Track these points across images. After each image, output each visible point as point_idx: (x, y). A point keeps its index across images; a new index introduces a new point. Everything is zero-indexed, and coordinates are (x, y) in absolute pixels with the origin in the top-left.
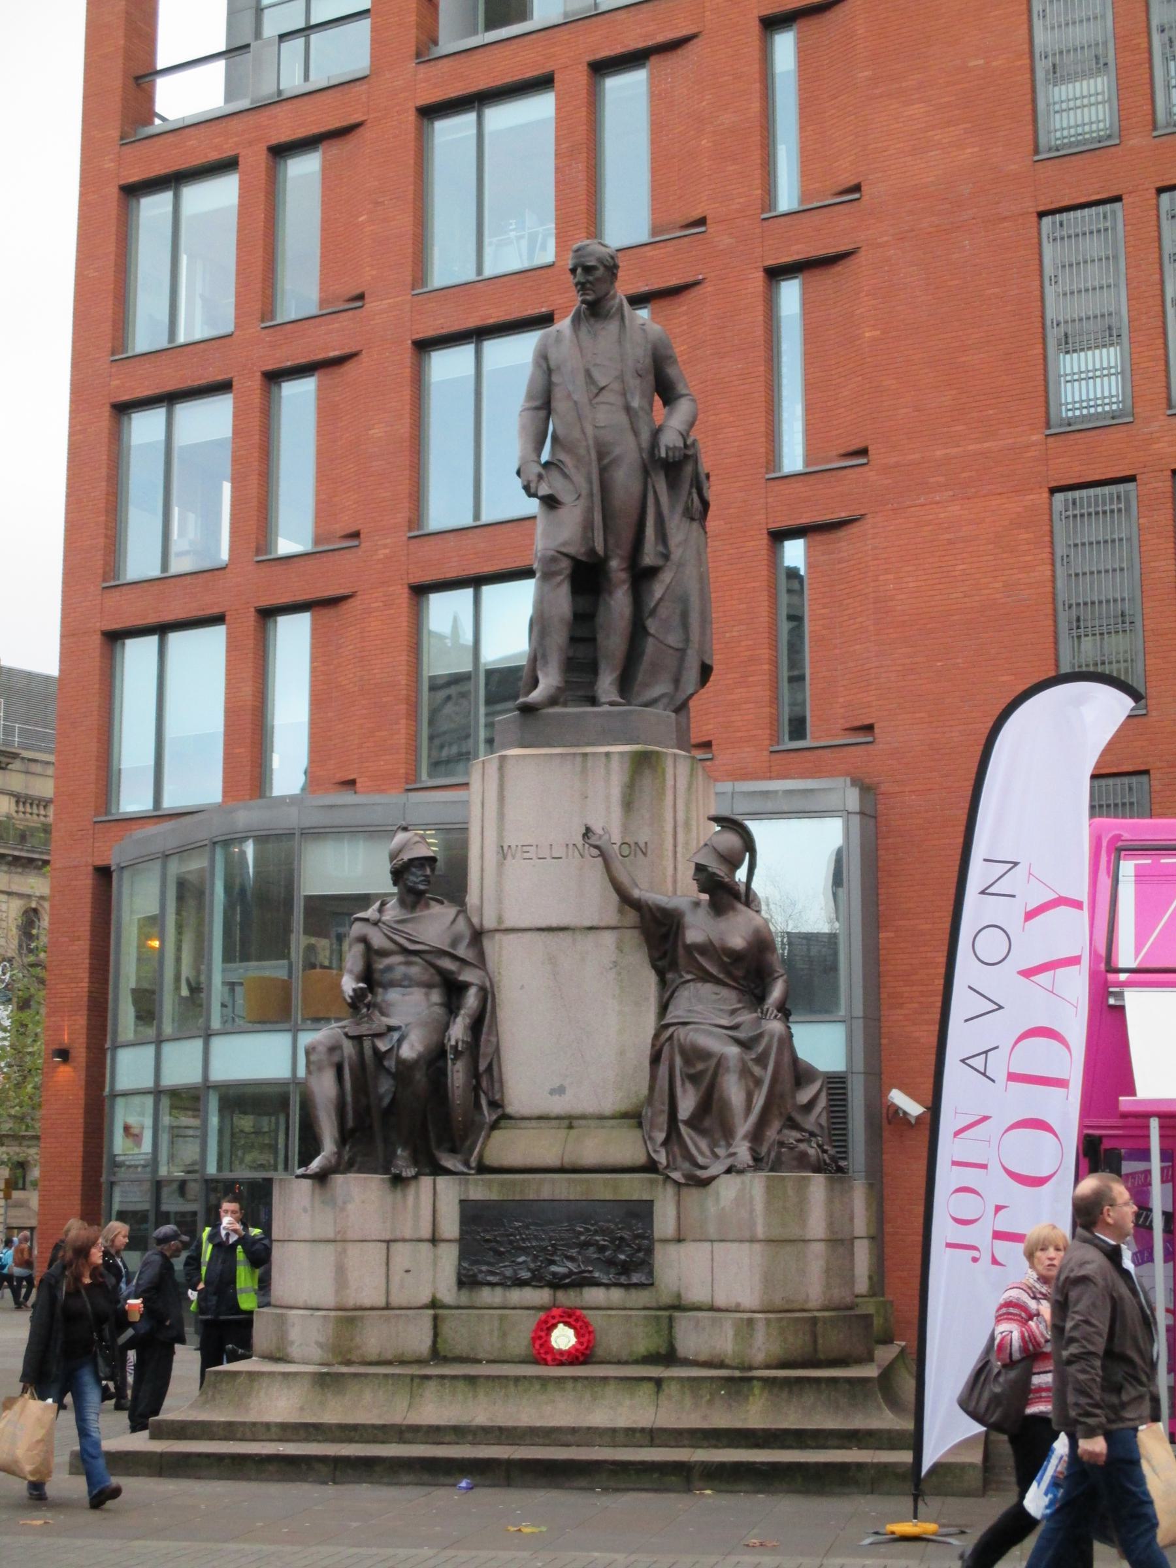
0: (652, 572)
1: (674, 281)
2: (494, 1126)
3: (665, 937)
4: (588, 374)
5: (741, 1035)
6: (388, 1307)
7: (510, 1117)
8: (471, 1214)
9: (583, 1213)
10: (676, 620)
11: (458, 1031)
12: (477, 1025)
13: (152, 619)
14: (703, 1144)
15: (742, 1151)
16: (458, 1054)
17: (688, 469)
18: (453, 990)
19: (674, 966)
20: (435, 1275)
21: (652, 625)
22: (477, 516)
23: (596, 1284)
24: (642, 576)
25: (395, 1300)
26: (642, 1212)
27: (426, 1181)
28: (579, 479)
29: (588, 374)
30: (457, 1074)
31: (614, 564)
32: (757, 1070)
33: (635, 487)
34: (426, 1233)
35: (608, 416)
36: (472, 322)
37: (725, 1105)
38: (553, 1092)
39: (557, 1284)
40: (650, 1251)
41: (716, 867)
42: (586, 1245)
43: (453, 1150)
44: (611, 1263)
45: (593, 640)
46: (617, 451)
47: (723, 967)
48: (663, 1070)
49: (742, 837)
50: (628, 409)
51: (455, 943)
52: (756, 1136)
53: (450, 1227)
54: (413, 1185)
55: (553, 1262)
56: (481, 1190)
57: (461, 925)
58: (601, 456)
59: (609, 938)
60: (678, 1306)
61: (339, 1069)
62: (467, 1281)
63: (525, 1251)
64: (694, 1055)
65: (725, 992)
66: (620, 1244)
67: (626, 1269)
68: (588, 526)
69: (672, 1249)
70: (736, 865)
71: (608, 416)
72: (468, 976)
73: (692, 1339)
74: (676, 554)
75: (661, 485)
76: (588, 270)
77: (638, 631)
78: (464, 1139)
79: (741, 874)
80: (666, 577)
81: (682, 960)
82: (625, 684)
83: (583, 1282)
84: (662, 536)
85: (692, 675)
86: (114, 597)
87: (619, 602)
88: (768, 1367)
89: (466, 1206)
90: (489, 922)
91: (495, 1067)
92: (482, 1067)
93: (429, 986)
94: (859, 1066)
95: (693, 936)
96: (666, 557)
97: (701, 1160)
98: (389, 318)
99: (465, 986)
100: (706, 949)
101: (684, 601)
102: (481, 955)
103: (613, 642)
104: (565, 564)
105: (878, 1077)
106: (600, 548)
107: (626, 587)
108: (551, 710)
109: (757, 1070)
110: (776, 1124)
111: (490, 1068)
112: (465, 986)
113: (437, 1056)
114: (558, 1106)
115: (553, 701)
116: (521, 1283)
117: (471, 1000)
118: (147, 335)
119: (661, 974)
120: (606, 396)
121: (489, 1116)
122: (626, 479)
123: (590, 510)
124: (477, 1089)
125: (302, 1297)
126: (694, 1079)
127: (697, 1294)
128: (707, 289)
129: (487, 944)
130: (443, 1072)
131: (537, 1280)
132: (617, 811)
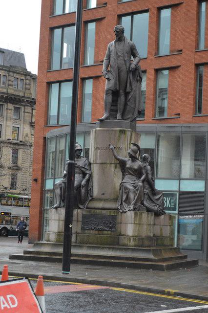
0: (129, 93)
1: (176, 3)
2: (91, 200)
3: (123, 166)
5: (134, 185)
8: (84, 216)
9: (104, 217)
10: (133, 102)
11: (84, 182)
12: (88, 181)
13: (57, 79)
14: (126, 205)
15: (132, 208)
16: (83, 187)
17: (137, 71)
18: (84, 174)
19: (125, 171)
24: (127, 94)
28: (114, 75)
30: (83, 190)
31: (121, 91)
32: (136, 192)
33: (126, 76)
35: (121, 61)
36: (131, 11)
37: (130, 198)
39: (98, 230)
41: (132, 154)
42: (104, 223)
43: (82, 205)
44: (108, 227)
45: (117, 106)
46: (122, 69)
47: (133, 172)
48: (121, 190)
50: (124, 60)
51: (85, 165)
52: (135, 204)
57: (87, 162)
58: (118, 70)
60: (120, 235)
61: (61, 188)
62: (83, 229)
63: (92, 223)
64: (126, 188)
65: (134, 177)
67: (111, 228)
68: (115, 84)
69: (120, 225)
70: (136, 153)
71: (121, 61)
75: (131, 76)
76: (117, 32)
77: (126, 104)
78: (84, 203)
80: (132, 93)
81: (126, 170)
82: (123, 115)
84: (131, 85)
85: (136, 113)
86: (49, 74)
87: (122, 98)
88: (133, 246)
90: (92, 162)
92: (89, 189)
95: (128, 166)
96: (132, 90)
97: (125, 208)
99: (87, 174)
100: (130, 168)
102: (91, 168)
103: (120, 106)
104: (110, 92)
106: (118, 89)
108: (107, 121)
109: (136, 192)
110: (140, 202)
112: (87, 174)
113: (80, 186)
115: (107, 118)
117: (87, 177)
118: (58, 11)
119: (122, 172)
120: (120, 58)
121: (90, 198)
122: (124, 75)
125: (53, 230)
126: (126, 193)
128: (184, 4)
129: (92, 166)
130: (80, 190)
131: (95, 229)
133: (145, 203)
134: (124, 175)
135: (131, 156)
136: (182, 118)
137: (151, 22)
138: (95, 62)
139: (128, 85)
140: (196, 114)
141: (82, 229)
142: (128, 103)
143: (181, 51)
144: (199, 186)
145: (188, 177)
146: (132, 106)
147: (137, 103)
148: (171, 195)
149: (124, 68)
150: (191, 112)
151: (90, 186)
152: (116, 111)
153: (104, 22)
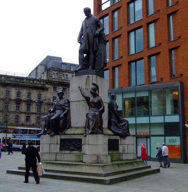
4: (86, 25)
6: (50, 153)
7: (72, 127)
8: (62, 140)
16: (61, 119)
20: (57, 148)
21: (97, 59)
22: (135, 52)
23: (75, 150)
24: (95, 52)
25: (51, 152)
26: (80, 140)
27: (56, 136)
29: (86, 25)
30: (61, 121)
31: (90, 51)
34: (56, 143)
38: (76, 124)
40: (82, 146)
45: (89, 62)
47: (94, 105)
49: (95, 86)
50: (91, 29)
51: (65, 104)
52: (93, 129)
53: (59, 142)
54: (54, 137)
55: (70, 147)
56: (63, 137)
59: (83, 102)
62: (61, 149)
66: (78, 145)
68: (85, 46)
70: (96, 91)
72: (67, 108)
73: (85, 159)
74: (100, 48)
77: (95, 60)
79: (97, 92)
83: (73, 150)
89: (61, 139)
91: (69, 120)
92: (67, 120)
93: (61, 110)
94: (181, 121)
95: (91, 101)
96: (98, 49)
98: (126, 29)
99: (66, 109)
100: (92, 102)
101: (101, 54)
105: (184, 123)
106: (88, 49)
107: (92, 54)
111: (68, 121)
112: (66, 109)
113: (58, 119)
114: (77, 126)
115: (80, 70)
116: (67, 150)
117: (66, 112)
120: (88, 28)
122: (91, 39)
123: (86, 44)
124: (66, 124)
127: (86, 153)
132: (85, 85)
133: (112, 128)
134: (90, 108)
135: (92, 93)
136: (164, 80)
137: (144, 32)
138: (118, 58)
139: (95, 46)
140: (172, 77)
141: (60, 150)
142: (96, 58)
143: (161, 43)
144: (175, 119)
145: (170, 114)
146: (100, 60)
147: (103, 58)
148: (158, 125)
149: (91, 35)
150: (169, 77)
151: (68, 118)
152: (89, 66)
153: (122, 36)
